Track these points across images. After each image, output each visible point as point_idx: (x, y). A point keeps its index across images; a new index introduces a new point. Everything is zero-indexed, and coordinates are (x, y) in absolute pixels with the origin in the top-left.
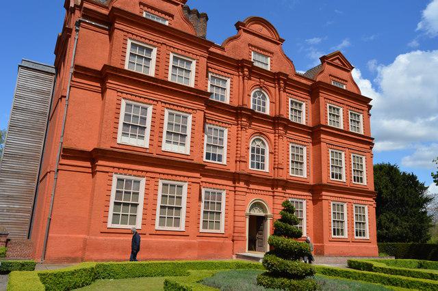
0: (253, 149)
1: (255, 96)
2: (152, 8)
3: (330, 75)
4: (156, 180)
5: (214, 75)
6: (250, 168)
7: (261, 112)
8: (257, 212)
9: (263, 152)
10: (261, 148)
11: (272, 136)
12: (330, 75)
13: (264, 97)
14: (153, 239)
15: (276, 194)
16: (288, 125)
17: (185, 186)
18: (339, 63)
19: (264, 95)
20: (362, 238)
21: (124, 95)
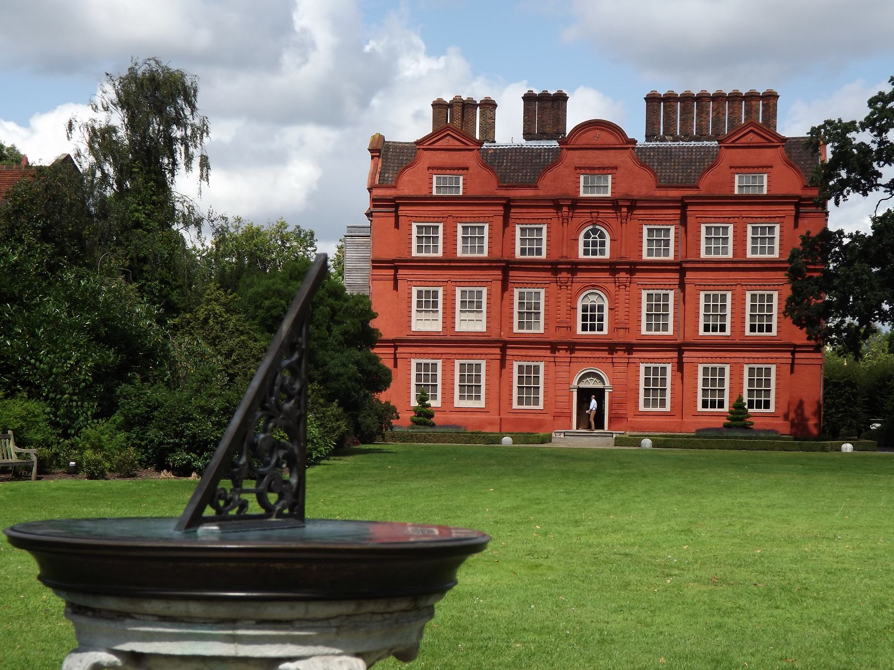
0: (585, 309)
1: (587, 236)
2: (442, 168)
3: (731, 167)
4: (452, 361)
5: (524, 226)
6: (579, 331)
8: (591, 384)
9: (601, 308)
10: (597, 304)
11: (611, 287)
12: (731, 167)
13: (602, 236)
14: (453, 416)
15: (631, 360)
16: (634, 267)
17: (483, 363)
18: (758, 139)
19: (602, 232)
20: (763, 410)
21: (414, 283)
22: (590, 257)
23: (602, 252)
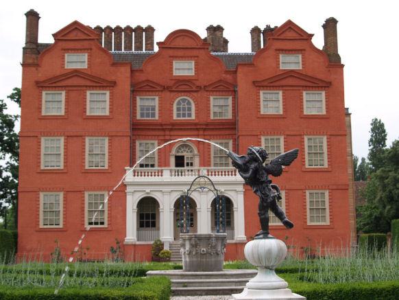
1: (179, 103)
7: (187, 118)
13: (189, 103)
19: (189, 101)
22: (182, 118)
23: (190, 115)
